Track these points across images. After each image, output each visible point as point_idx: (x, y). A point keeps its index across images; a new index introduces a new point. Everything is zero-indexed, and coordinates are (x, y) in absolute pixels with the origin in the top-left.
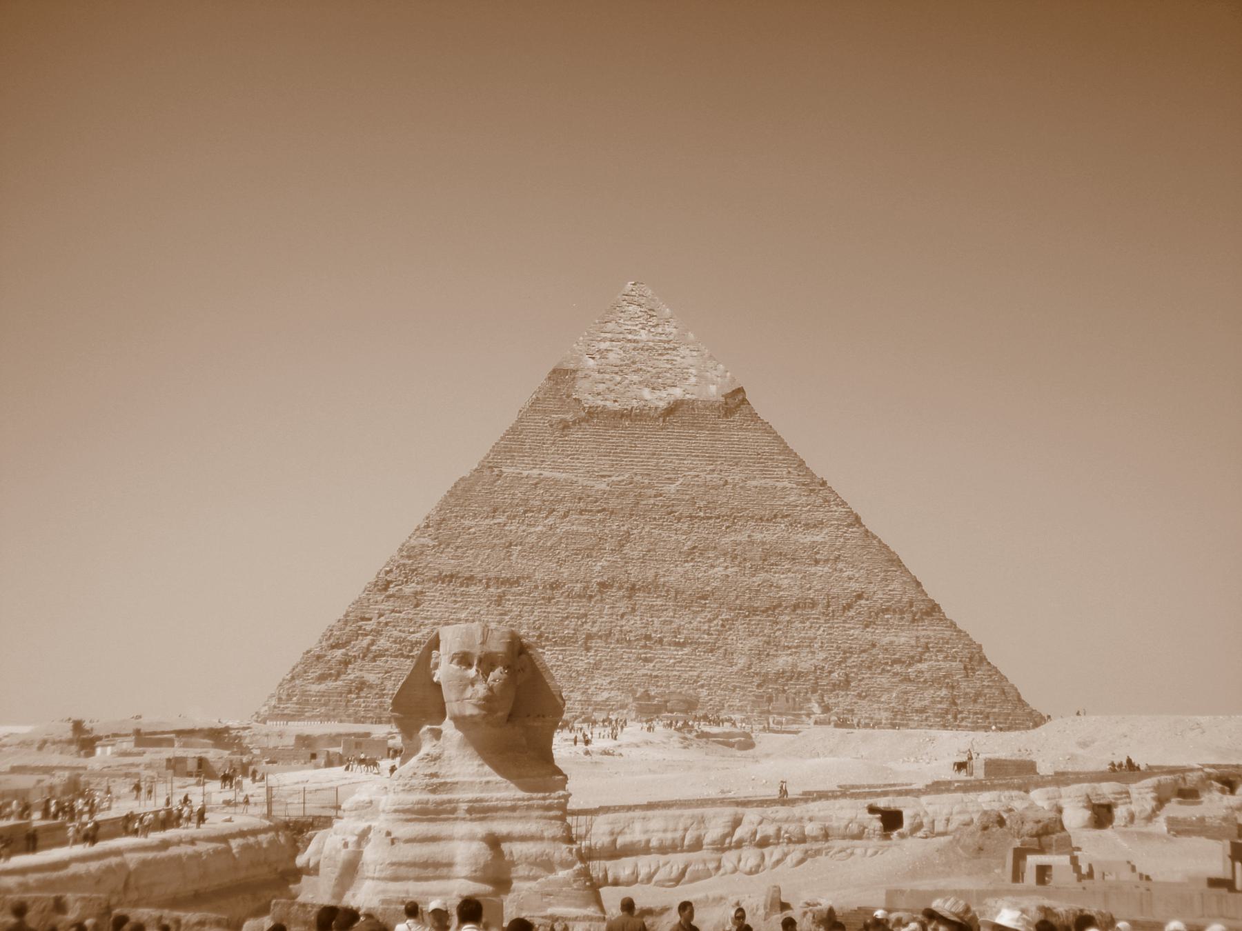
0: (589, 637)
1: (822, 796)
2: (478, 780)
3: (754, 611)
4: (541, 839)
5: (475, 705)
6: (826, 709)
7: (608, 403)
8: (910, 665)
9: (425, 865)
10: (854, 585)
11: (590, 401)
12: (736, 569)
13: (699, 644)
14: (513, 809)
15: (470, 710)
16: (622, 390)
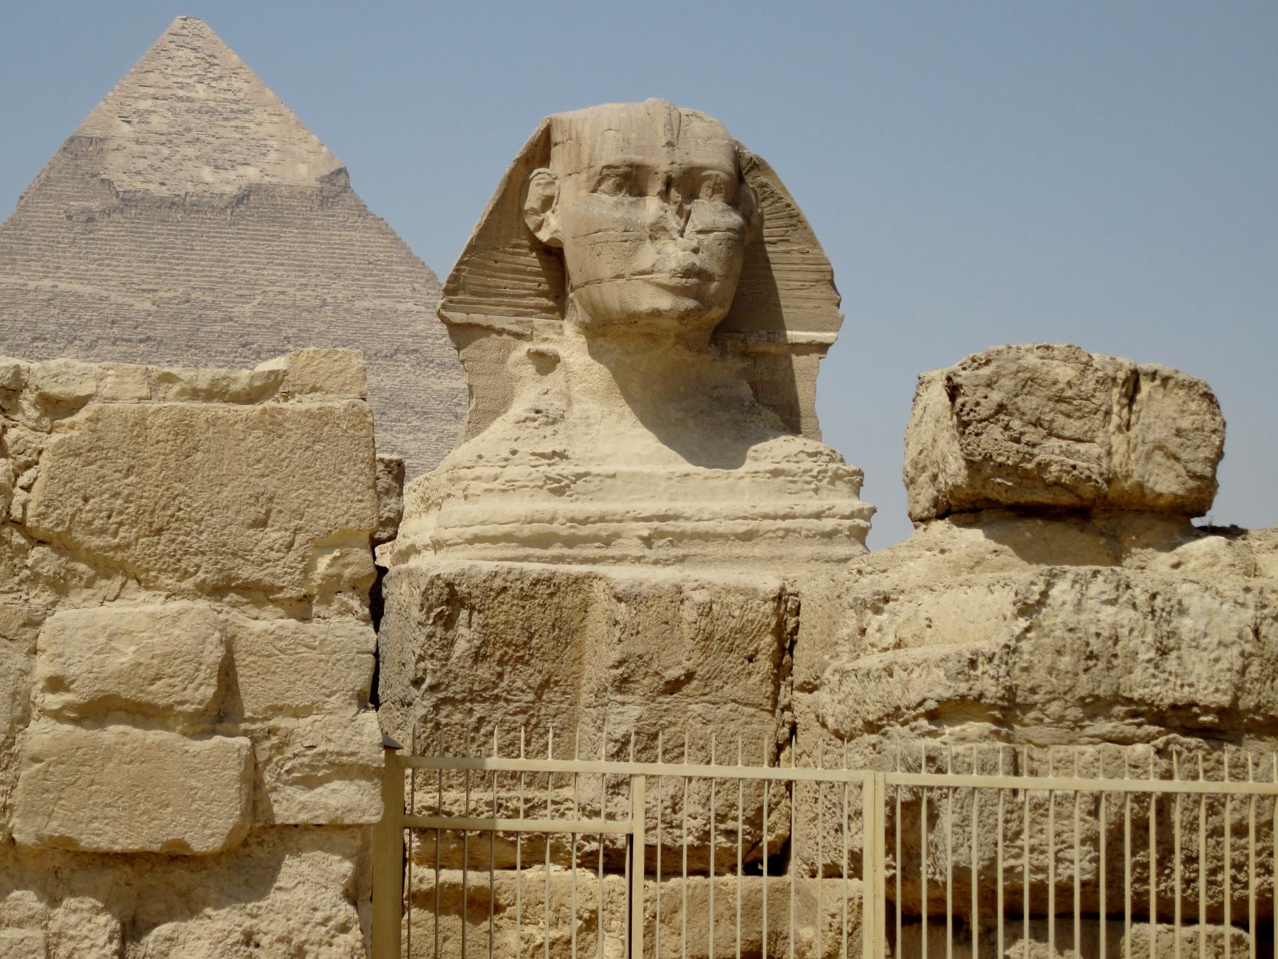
2: (662, 470)
7: (151, 187)
11: (125, 183)
14: (748, 536)
15: (651, 300)
16: (172, 169)
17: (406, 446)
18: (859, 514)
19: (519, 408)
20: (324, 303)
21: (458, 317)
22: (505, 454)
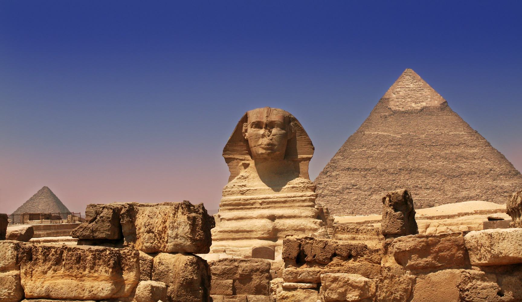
1: (466, 214)
3: (454, 176)
4: (300, 217)
5: (263, 148)
7: (400, 109)
9: (237, 232)
10: (489, 167)
11: (394, 108)
14: (285, 202)
15: (261, 151)
18: (312, 195)
19: (239, 177)
20: (442, 133)
21: (227, 156)
22: (232, 186)
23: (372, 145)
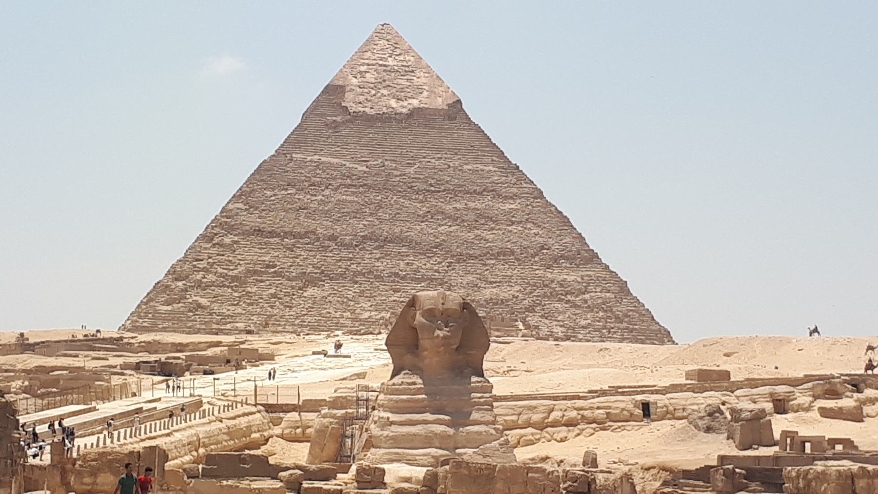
0: (356, 274)
3: (471, 255)
6: (527, 327)
7: (367, 110)
8: (577, 296)
11: (353, 108)
12: (457, 227)
13: (432, 280)
16: (376, 100)
17: (487, 237)
20: (449, 166)
23: (306, 184)
